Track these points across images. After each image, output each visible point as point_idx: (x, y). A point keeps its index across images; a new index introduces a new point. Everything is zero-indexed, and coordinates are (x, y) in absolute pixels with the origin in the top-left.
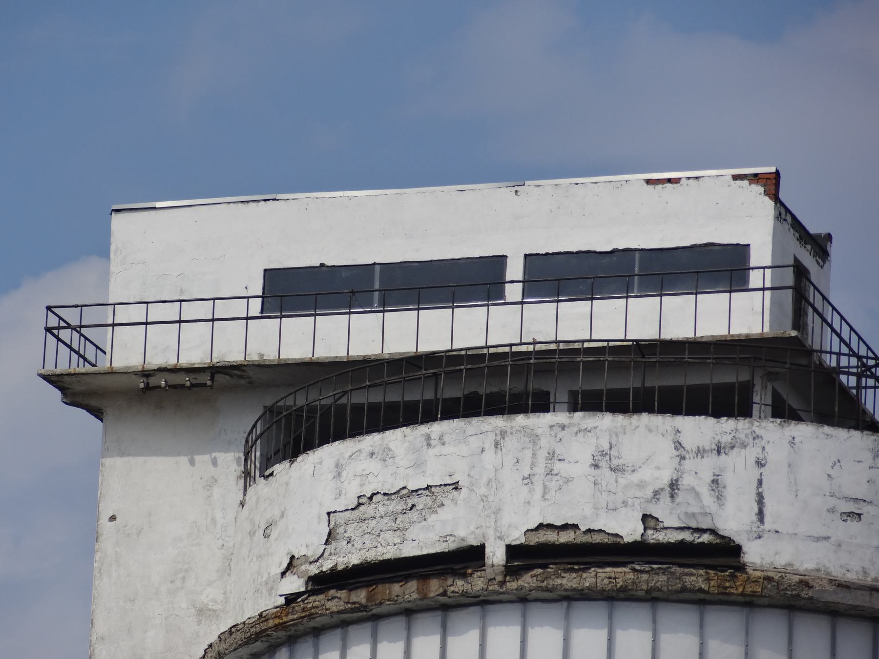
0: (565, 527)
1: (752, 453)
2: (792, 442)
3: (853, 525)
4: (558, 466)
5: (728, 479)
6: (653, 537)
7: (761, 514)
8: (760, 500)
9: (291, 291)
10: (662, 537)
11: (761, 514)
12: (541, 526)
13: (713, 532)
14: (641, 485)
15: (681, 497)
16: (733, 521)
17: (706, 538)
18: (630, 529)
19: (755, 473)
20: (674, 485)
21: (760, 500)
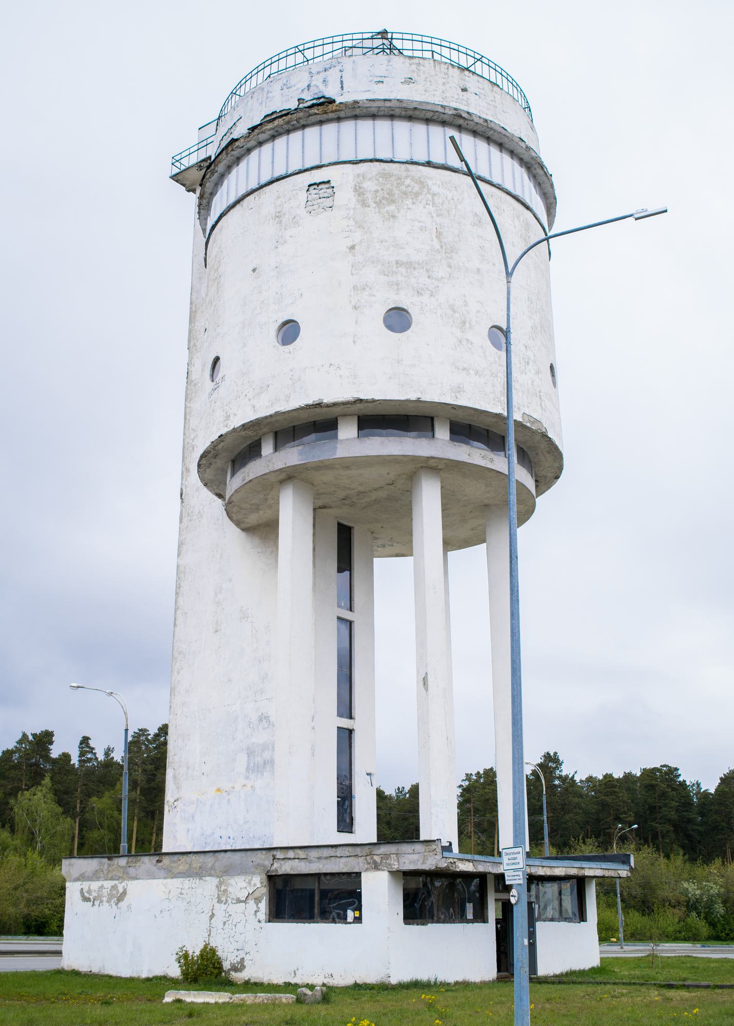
0: (273, 113)
1: (339, 67)
2: (354, 62)
3: (380, 85)
4: (270, 95)
5: (330, 79)
6: (301, 106)
7: (342, 87)
8: (342, 82)
10: (306, 105)
11: (342, 87)
12: (265, 117)
13: (323, 97)
14: (298, 89)
15: (312, 89)
16: (331, 92)
17: (322, 100)
18: (293, 105)
19: (340, 74)
20: (309, 86)
21: (342, 82)
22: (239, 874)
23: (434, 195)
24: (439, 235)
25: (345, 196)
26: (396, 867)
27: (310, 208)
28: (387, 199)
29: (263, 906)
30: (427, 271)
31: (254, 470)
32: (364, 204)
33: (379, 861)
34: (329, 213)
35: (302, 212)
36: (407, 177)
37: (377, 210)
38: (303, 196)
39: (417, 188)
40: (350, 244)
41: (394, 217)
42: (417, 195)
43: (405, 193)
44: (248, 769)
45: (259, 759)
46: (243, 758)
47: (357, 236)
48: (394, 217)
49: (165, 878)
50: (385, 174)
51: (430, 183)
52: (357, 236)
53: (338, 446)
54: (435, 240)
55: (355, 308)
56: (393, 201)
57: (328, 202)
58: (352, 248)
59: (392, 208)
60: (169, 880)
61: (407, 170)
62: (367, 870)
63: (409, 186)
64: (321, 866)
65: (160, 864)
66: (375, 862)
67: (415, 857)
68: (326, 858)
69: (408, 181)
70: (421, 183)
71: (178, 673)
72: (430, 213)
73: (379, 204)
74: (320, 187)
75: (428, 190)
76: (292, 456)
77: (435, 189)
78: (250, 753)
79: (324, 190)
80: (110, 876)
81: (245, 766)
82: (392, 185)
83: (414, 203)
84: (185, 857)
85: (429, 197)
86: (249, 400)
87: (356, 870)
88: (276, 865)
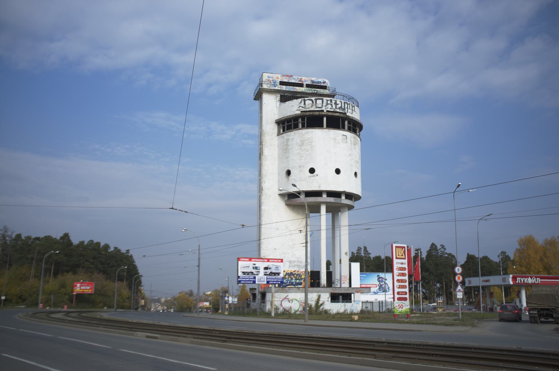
9: (282, 83)
31: (318, 199)
35: (340, 141)
38: (341, 137)
76: (332, 200)
78: (290, 262)
79: (345, 137)
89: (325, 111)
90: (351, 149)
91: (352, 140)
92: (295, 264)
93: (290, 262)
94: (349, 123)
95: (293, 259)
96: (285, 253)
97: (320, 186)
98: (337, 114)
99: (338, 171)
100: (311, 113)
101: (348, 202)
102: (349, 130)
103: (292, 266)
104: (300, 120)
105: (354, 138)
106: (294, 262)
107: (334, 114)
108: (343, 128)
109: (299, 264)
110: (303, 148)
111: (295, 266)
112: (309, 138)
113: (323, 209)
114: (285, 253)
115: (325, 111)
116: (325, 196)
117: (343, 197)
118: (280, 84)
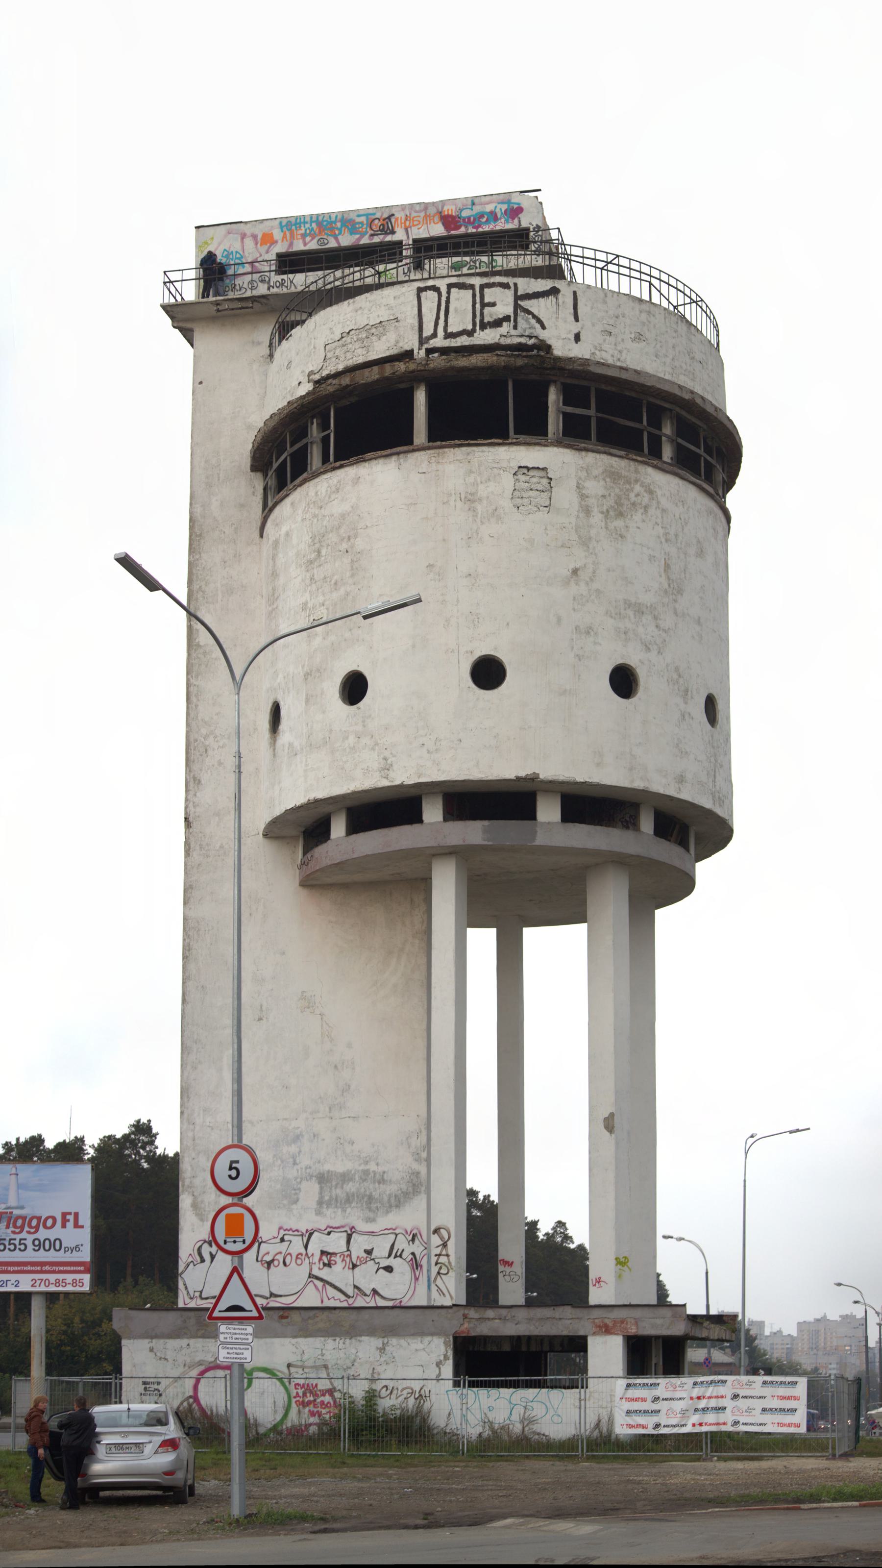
22: (413, 1335)
23: (664, 511)
24: (667, 567)
25: (565, 496)
26: (633, 1331)
27: (519, 501)
28: (615, 510)
29: (448, 1370)
30: (656, 618)
32: (587, 511)
33: (611, 1325)
34: (542, 515)
35: (506, 504)
36: (637, 481)
37: (603, 524)
39: (646, 499)
40: (572, 566)
41: (622, 536)
42: (646, 508)
43: (634, 504)
44: (320, 1203)
45: (339, 1191)
46: (310, 1191)
47: (579, 557)
48: (622, 536)
49: (295, 1337)
50: (613, 473)
51: (659, 493)
52: (579, 557)
53: (538, 829)
54: (663, 575)
55: (579, 657)
56: (620, 515)
57: (543, 499)
58: (575, 572)
59: (619, 523)
60: (300, 1340)
61: (637, 471)
62: (594, 1334)
63: (637, 495)
64: (532, 1328)
65: (284, 1321)
66: (606, 1326)
67: (659, 1322)
68: (541, 1319)
69: (638, 488)
70: (651, 492)
71: (195, 1068)
72: (659, 537)
73: (606, 514)
74: (531, 473)
75: (658, 503)
76: (473, 832)
77: (664, 502)
79: (535, 479)
80: (200, 1334)
81: (317, 1199)
82: (621, 490)
83: (644, 521)
84: (326, 1313)
85: (659, 512)
86: (429, 752)
87: (581, 1333)
88: (466, 1325)
89: (420, 354)
90: (585, 542)
91: (595, 487)
92: (351, 1187)
93: (323, 1179)
94: (571, 396)
95: (339, 1166)
96: (297, 1138)
97: (387, 768)
98: (476, 360)
99: (488, 673)
100: (346, 381)
101: (586, 837)
102: (575, 433)
103: (334, 1202)
104: (314, 431)
105: (613, 476)
106: (345, 1177)
107: (462, 362)
108: (532, 428)
109: (370, 1187)
110: (319, 574)
111: (349, 1200)
112: (343, 516)
113: (445, 890)
114: (297, 1138)
115: (420, 354)
116: (433, 813)
117: (548, 812)
118: (280, 271)
